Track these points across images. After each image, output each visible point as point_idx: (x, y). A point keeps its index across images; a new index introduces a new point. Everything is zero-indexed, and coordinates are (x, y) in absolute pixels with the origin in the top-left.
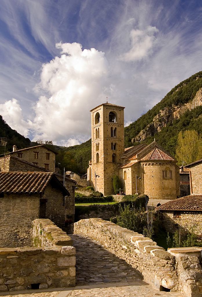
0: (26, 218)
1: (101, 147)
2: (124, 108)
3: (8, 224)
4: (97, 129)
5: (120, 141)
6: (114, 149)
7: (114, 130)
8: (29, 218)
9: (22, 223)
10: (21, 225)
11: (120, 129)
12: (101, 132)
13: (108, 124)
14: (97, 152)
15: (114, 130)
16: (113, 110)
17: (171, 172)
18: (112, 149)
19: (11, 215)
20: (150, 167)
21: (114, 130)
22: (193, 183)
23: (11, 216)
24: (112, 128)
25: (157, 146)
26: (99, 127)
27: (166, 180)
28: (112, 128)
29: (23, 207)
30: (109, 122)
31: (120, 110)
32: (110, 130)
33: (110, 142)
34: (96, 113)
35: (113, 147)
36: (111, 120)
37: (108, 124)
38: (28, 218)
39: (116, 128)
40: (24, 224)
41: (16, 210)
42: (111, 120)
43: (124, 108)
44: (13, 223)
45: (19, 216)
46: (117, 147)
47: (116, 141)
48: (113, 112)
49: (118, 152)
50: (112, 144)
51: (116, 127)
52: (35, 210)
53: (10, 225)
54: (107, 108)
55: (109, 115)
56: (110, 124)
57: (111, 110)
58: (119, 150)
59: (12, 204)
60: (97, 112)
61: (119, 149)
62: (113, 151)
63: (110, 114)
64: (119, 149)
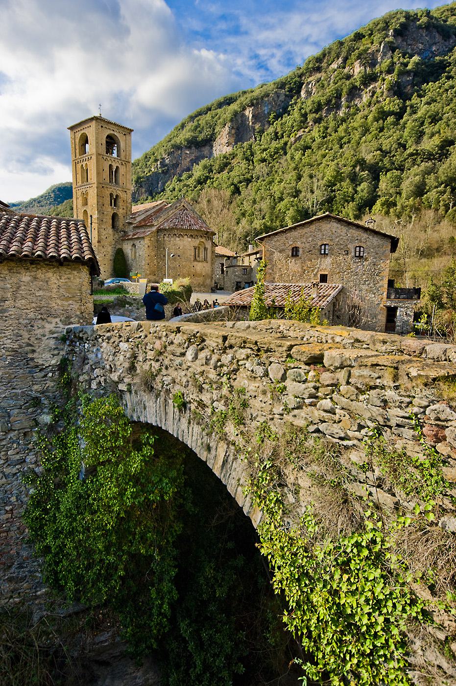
0: (49, 319)
2: (133, 130)
3: (3, 335)
7: (114, 171)
8: (58, 320)
9: (40, 330)
10: (39, 336)
11: (125, 170)
12: (92, 171)
13: (105, 158)
14: (85, 209)
16: (112, 132)
17: (206, 249)
18: (111, 205)
19: (10, 313)
21: (114, 171)
23: (11, 315)
24: (111, 166)
27: (199, 261)
28: (111, 166)
29: (41, 293)
30: (105, 154)
31: (125, 135)
32: (107, 169)
33: (107, 193)
34: (78, 135)
36: (109, 150)
38: (54, 320)
39: (117, 167)
40: (47, 334)
41: (24, 301)
42: (109, 150)
43: (133, 130)
44: (17, 331)
45: (32, 315)
46: (120, 203)
47: (118, 191)
48: (113, 136)
49: (121, 212)
50: (111, 195)
52: (71, 302)
53: (9, 337)
54: (102, 127)
55: (106, 141)
56: (109, 159)
57: (109, 130)
59: (9, 286)
60: (82, 132)
61: (122, 205)
62: (112, 208)
63: (108, 140)
64: (122, 205)
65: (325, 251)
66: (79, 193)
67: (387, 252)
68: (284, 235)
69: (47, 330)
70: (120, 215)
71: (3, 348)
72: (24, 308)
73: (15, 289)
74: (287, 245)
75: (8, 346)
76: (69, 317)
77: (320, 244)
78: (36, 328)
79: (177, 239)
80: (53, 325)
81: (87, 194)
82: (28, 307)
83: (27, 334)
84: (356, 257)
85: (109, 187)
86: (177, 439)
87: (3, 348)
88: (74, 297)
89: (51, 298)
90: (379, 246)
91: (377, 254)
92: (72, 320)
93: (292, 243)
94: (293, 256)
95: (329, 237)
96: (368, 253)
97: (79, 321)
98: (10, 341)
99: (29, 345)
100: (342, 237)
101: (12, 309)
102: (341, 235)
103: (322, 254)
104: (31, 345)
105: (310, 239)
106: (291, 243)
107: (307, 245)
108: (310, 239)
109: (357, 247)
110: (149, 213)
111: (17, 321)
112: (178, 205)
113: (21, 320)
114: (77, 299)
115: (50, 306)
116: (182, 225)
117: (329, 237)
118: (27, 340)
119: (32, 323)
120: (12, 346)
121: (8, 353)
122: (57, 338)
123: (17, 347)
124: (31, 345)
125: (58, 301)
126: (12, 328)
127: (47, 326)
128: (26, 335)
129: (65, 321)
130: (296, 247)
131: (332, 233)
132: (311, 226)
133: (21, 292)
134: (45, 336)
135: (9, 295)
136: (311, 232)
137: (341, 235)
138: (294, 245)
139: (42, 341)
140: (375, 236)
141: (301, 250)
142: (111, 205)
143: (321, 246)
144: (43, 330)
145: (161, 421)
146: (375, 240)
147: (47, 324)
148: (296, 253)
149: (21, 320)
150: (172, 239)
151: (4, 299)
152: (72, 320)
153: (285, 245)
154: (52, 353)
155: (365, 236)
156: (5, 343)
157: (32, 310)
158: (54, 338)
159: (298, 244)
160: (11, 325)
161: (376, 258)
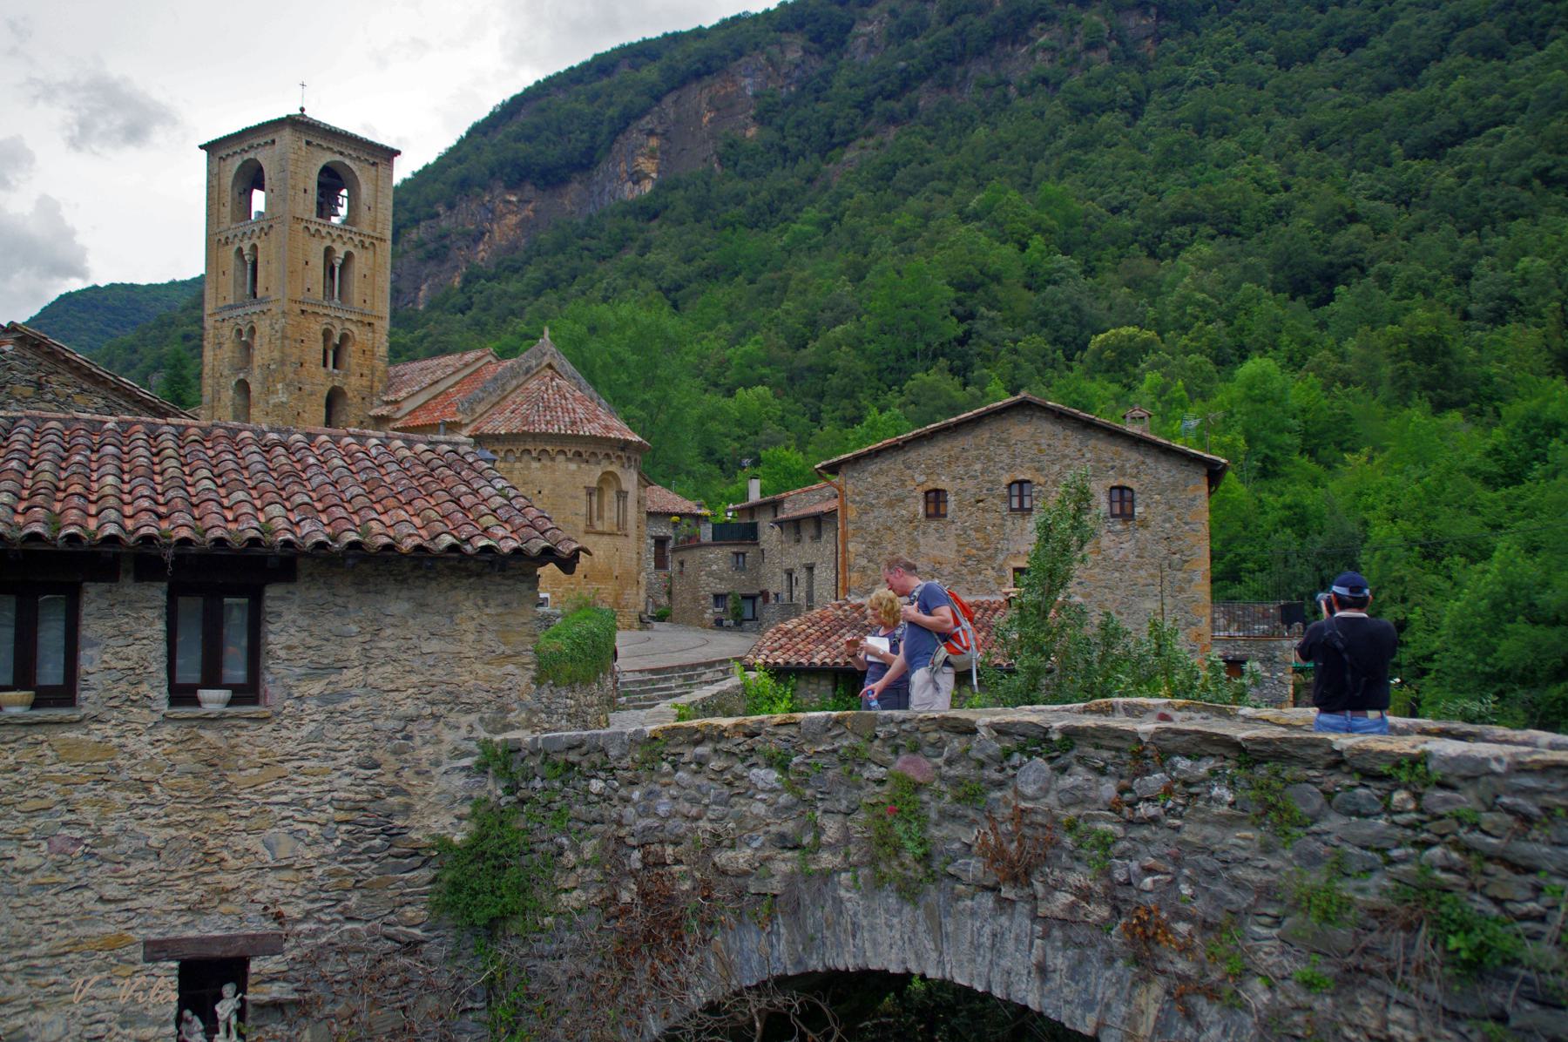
0: (452, 718)
1: (266, 351)
2: (398, 153)
3: (331, 764)
4: (246, 250)
5: (370, 324)
6: (335, 367)
8: (473, 717)
9: (429, 749)
10: (425, 765)
13: (313, 228)
14: (242, 376)
15: (338, 263)
16: (338, 158)
17: (622, 495)
18: (325, 365)
19: (354, 701)
20: (528, 468)
22: (851, 547)
23: (354, 707)
24: (329, 252)
25: (555, 364)
26: (255, 240)
27: (602, 534)
28: (329, 252)
29: (434, 645)
30: (314, 217)
31: (374, 164)
32: (318, 262)
33: (317, 328)
34: (234, 164)
35: (331, 354)
37: (313, 228)
38: (465, 720)
39: (349, 256)
40: (444, 758)
41: (389, 668)
43: (398, 153)
44: (367, 751)
45: (408, 708)
46: (352, 357)
47: (348, 325)
49: (353, 385)
50: (327, 334)
51: (350, 248)
52: (510, 668)
53: (347, 769)
54: (308, 143)
55: (320, 185)
56: (324, 231)
58: (358, 371)
59: (354, 628)
61: (359, 365)
62: (329, 374)
64: (359, 365)
65: (1021, 503)
66: (228, 331)
67: (1198, 502)
68: (900, 458)
69: (446, 747)
70: (350, 395)
71: (330, 803)
72: (391, 686)
73: (368, 637)
74: (910, 485)
75: (343, 795)
76: (504, 710)
77: (1006, 479)
78: (418, 741)
79: (535, 465)
80: (463, 732)
81: (253, 330)
82: (400, 683)
83: (392, 759)
84: (1113, 516)
85: (321, 311)
86: (987, 996)
87: (330, 803)
88: (518, 654)
89: (459, 657)
90: (1174, 487)
91: (1171, 508)
92: (512, 717)
93: (923, 478)
94: (928, 516)
95: (1032, 460)
96: (1148, 506)
97: (529, 720)
98: (348, 780)
99: (395, 791)
100: (1067, 461)
101: (358, 691)
102: (1065, 456)
103: (1012, 510)
104: (405, 793)
105: (978, 467)
106: (920, 480)
107: (969, 484)
108: (978, 467)
109: (1113, 488)
110: (441, 387)
111: (369, 725)
112: (534, 363)
113: (380, 722)
114: (527, 660)
115: (456, 680)
116: (548, 423)
117: (1032, 460)
118: (389, 778)
119: (409, 728)
120: (352, 795)
121: (341, 816)
122: (468, 768)
123: (365, 797)
124: (405, 793)
125: (477, 667)
126: (356, 744)
127: (449, 736)
128: (391, 763)
129: (494, 720)
130: (937, 491)
131: (1040, 451)
132: (978, 432)
133: (383, 644)
134: (437, 764)
135: (354, 652)
136: (977, 447)
137: (1065, 456)
138: (931, 485)
139: (431, 778)
140: (1163, 458)
141: (951, 498)
142: (325, 365)
143: (1010, 486)
144: (436, 748)
145: (918, 957)
146: (1164, 471)
147: (446, 731)
148: (937, 508)
149: (380, 722)
150: (518, 465)
151: (340, 665)
152: (512, 717)
153: (903, 483)
154: (457, 812)
155: (1133, 457)
156: (336, 786)
157: (410, 691)
158: (463, 769)
159: (943, 483)
160: (353, 737)
161: (1169, 520)
